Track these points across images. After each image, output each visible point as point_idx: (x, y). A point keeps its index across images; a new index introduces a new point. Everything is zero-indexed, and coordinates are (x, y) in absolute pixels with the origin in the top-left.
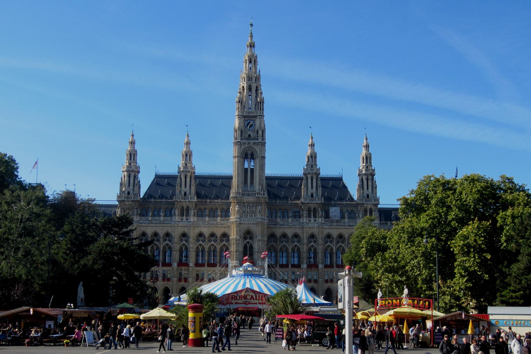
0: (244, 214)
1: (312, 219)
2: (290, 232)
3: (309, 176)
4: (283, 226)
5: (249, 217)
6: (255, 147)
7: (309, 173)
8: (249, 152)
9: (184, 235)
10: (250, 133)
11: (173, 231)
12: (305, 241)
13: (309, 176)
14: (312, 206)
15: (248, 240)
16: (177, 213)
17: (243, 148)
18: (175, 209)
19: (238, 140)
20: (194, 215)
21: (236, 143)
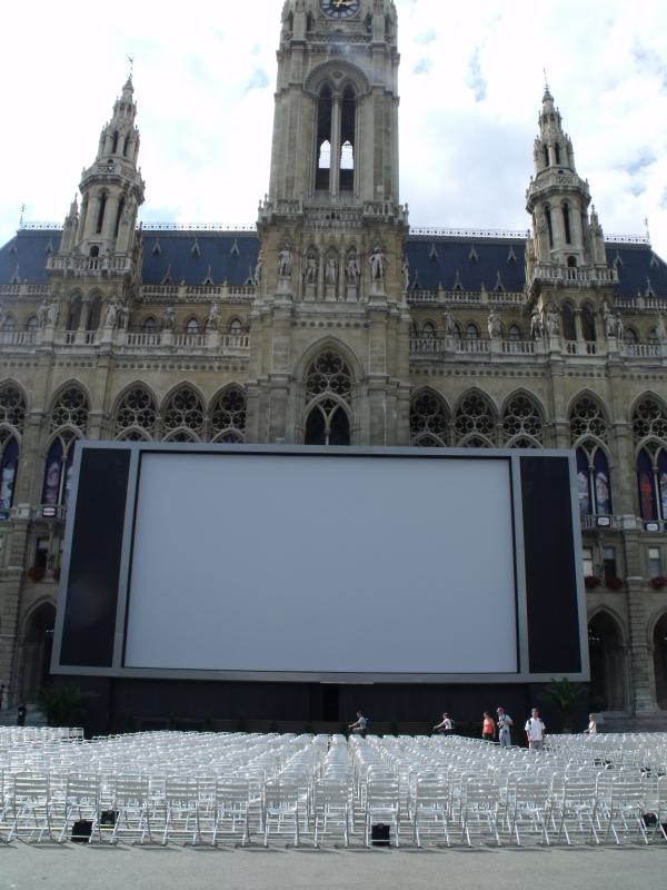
0: (310, 289)
1: (582, 348)
2: (498, 391)
3: (555, 201)
4: (469, 369)
7: (554, 191)
8: (337, 82)
9: (73, 398)
11: (30, 383)
12: (562, 419)
13: (555, 201)
14: (578, 300)
15: (328, 393)
16: (52, 315)
17: (312, 65)
18: (50, 302)
19: (294, 39)
20: (118, 324)
21: (284, 55)
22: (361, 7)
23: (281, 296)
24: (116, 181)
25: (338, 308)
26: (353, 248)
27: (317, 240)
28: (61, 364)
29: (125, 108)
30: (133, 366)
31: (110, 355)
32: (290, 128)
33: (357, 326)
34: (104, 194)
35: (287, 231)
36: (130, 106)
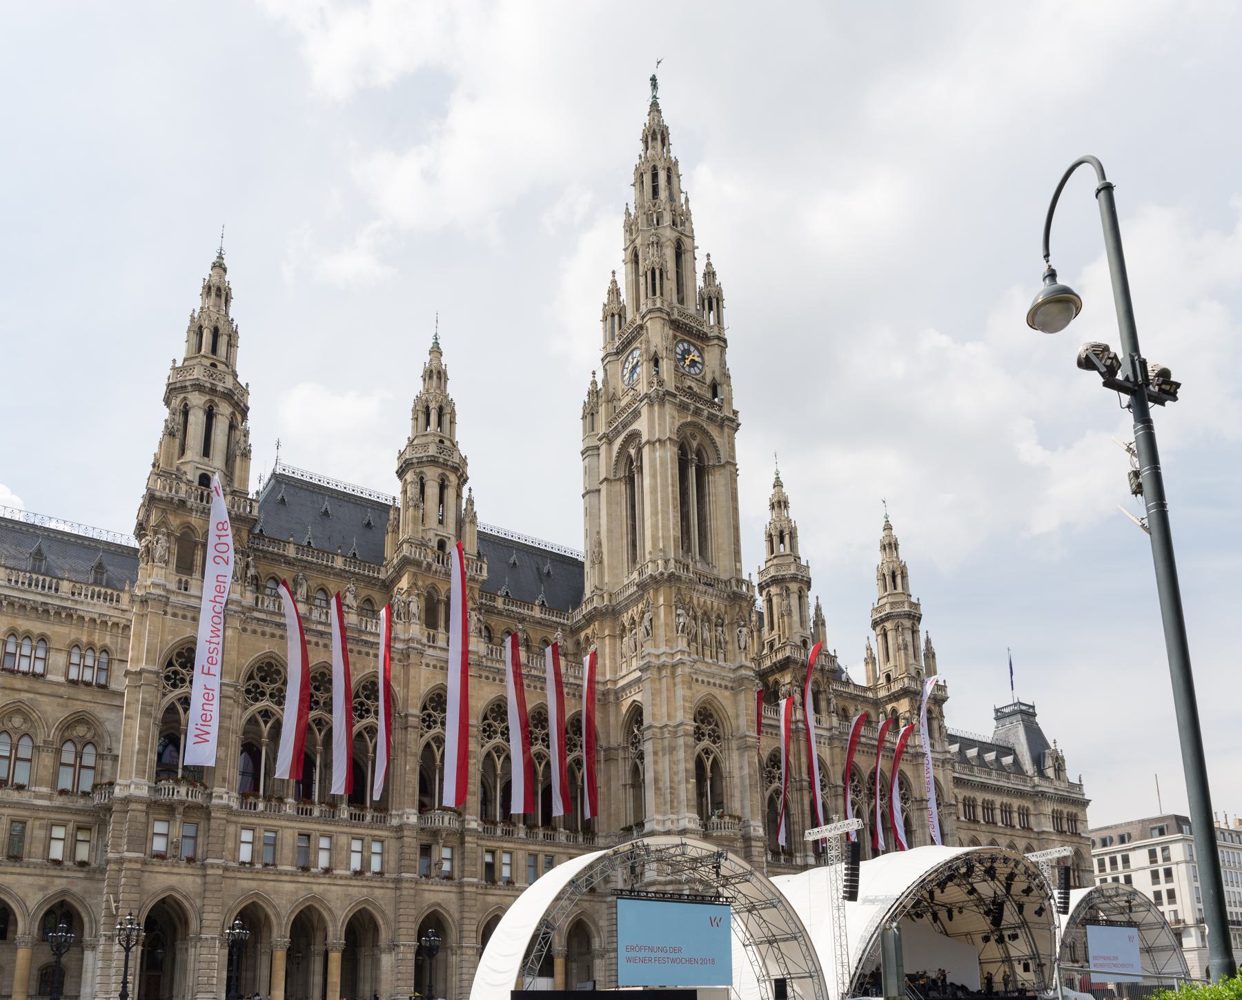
5: (708, 660)
6: (714, 432)
8: (695, 444)
10: (693, 385)
16: (413, 608)
22: (707, 369)
23: (683, 652)
24: (455, 469)
25: (714, 669)
26: (718, 616)
27: (695, 602)
28: (428, 665)
29: (436, 375)
30: (494, 679)
31: (479, 665)
32: (673, 486)
33: (726, 687)
34: (443, 480)
35: (679, 589)
36: (439, 372)
